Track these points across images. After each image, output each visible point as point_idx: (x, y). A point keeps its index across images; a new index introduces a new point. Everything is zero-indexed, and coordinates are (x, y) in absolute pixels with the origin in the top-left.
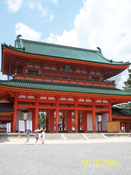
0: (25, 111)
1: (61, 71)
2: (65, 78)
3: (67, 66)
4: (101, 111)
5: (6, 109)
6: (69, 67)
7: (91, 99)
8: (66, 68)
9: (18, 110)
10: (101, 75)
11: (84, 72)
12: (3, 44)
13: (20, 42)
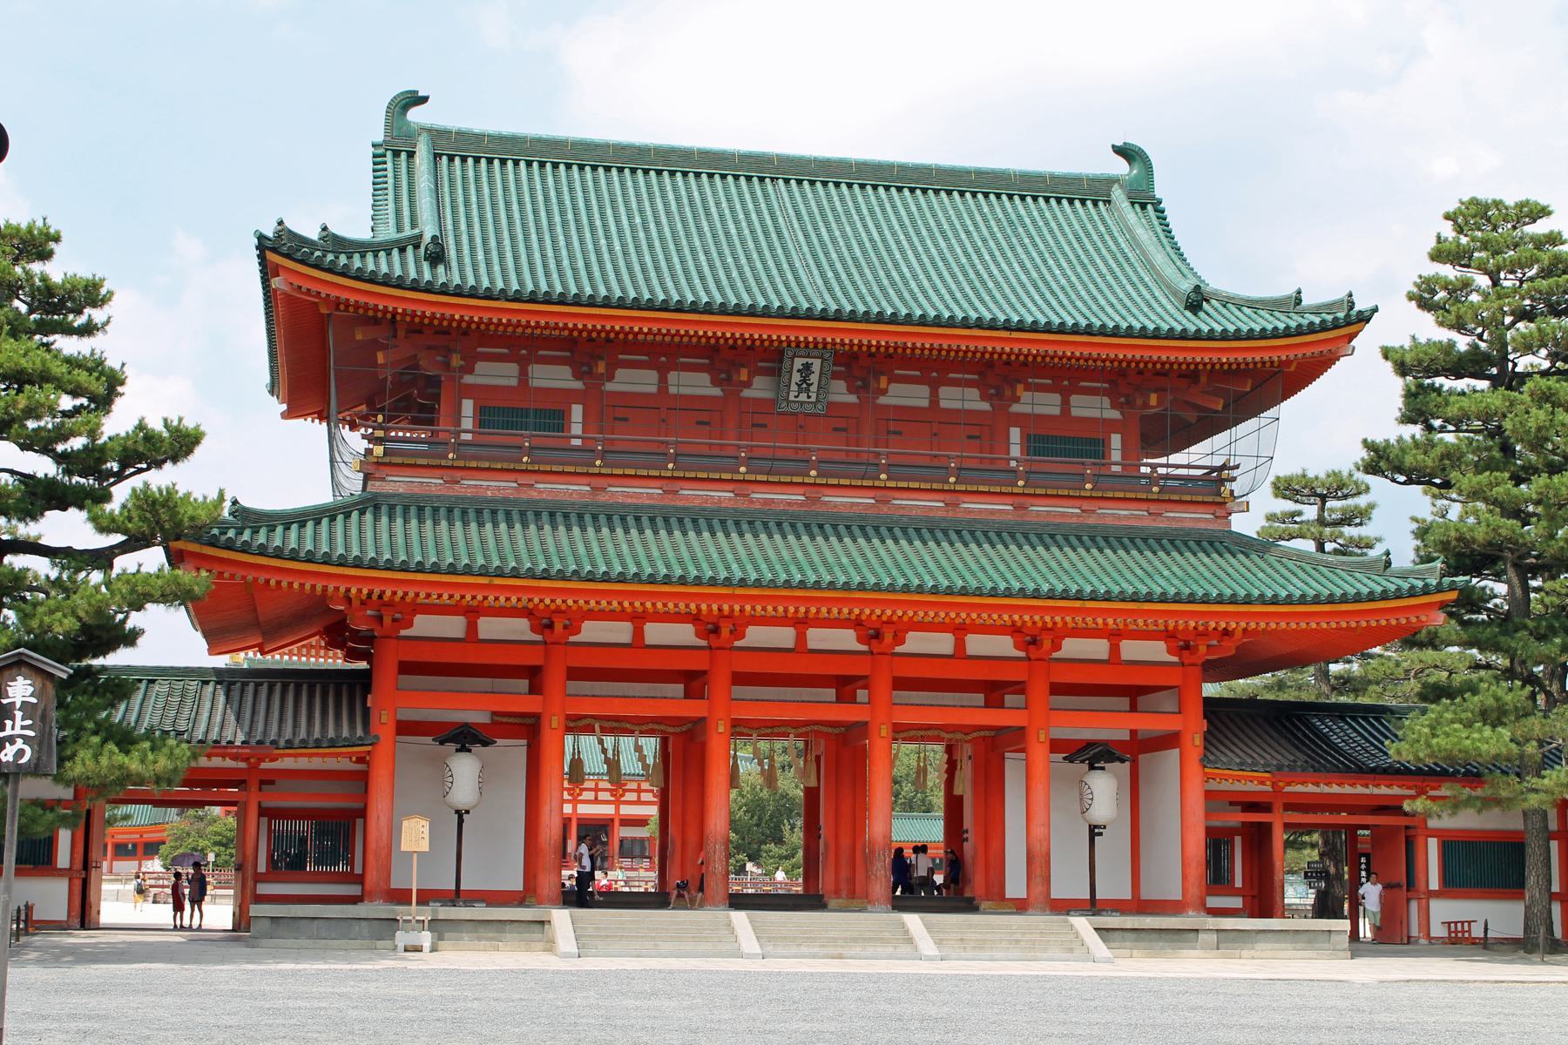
0: (465, 738)
1: (756, 400)
2: (774, 470)
3: (799, 363)
4: (1133, 733)
6: (816, 364)
8: (796, 377)
9: (406, 728)
10: (1115, 414)
11: (962, 398)
13: (411, 155)
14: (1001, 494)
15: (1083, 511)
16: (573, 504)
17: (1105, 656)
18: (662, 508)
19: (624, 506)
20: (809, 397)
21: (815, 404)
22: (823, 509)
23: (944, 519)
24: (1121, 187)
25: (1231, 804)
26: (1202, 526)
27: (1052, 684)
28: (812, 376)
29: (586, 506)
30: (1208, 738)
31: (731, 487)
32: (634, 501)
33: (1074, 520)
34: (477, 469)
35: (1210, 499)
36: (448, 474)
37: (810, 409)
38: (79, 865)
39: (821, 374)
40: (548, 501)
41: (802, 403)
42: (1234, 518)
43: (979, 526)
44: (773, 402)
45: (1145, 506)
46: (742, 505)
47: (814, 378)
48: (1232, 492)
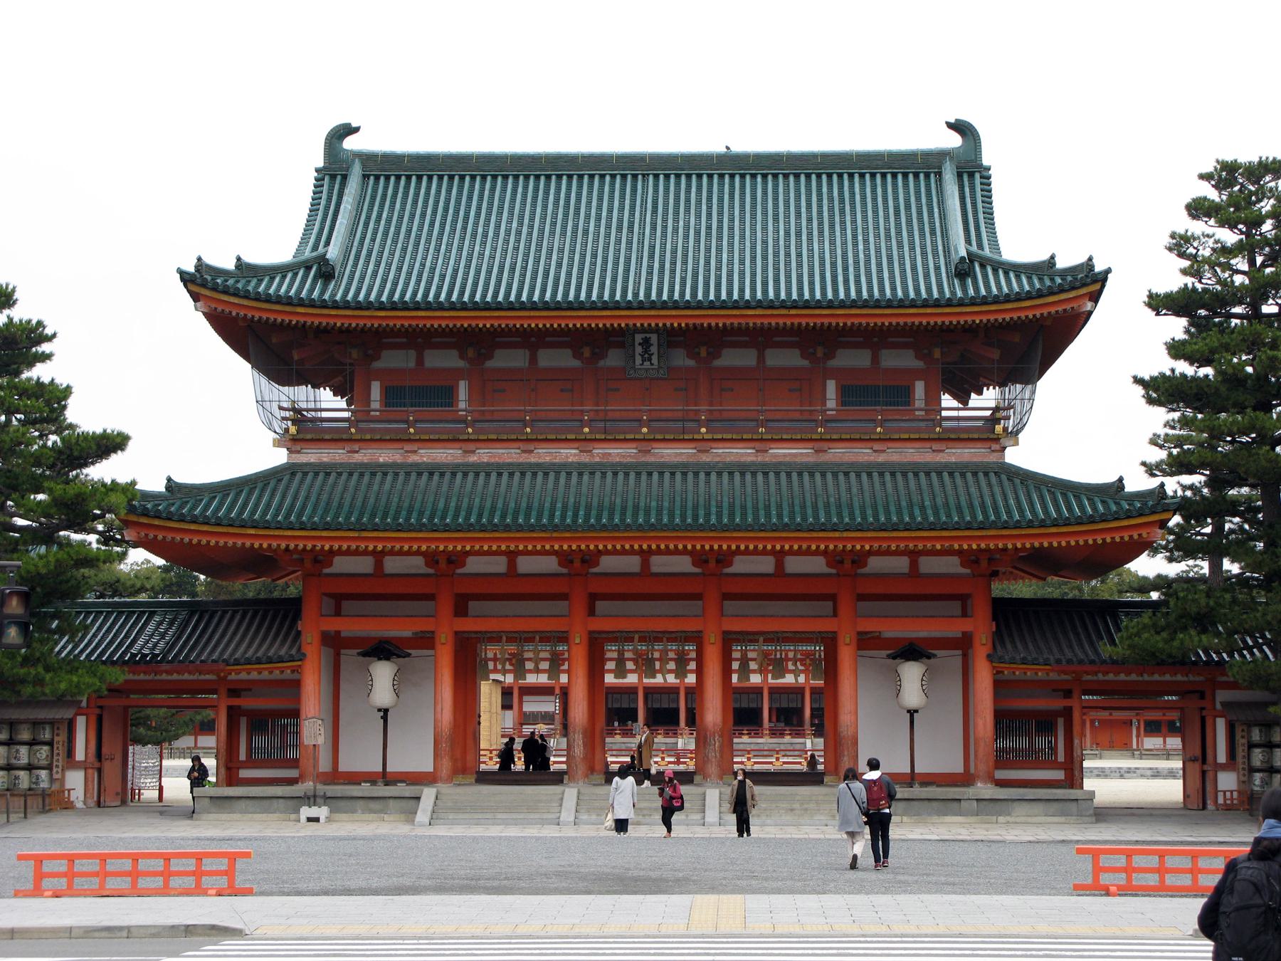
5: (271, 645)
6: (654, 338)
8: (639, 349)
11: (789, 358)
12: (191, 269)
16: (448, 464)
17: (906, 570)
18: (520, 464)
19: (488, 464)
20: (652, 364)
21: (658, 370)
22: (652, 459)
23: (753, 463)
24: (952, 159)
25: (1054, 690)
26: (980, 459)
27: (858, 595)
28: (652, 348)
29: (458, 465)
30: (998, 638)
31: (576, 445)
34: (371, 440)
35: (985, 436)
36: (348, 447)
38: (92, 758)
39: (659, 345)
40: (427, 464)
41: (647, 370)
42: (1008, 451)
43: (783, 467)
45: (928, 445)
46: (585, 458)
47: (654, 349)
48: (1005, 429)
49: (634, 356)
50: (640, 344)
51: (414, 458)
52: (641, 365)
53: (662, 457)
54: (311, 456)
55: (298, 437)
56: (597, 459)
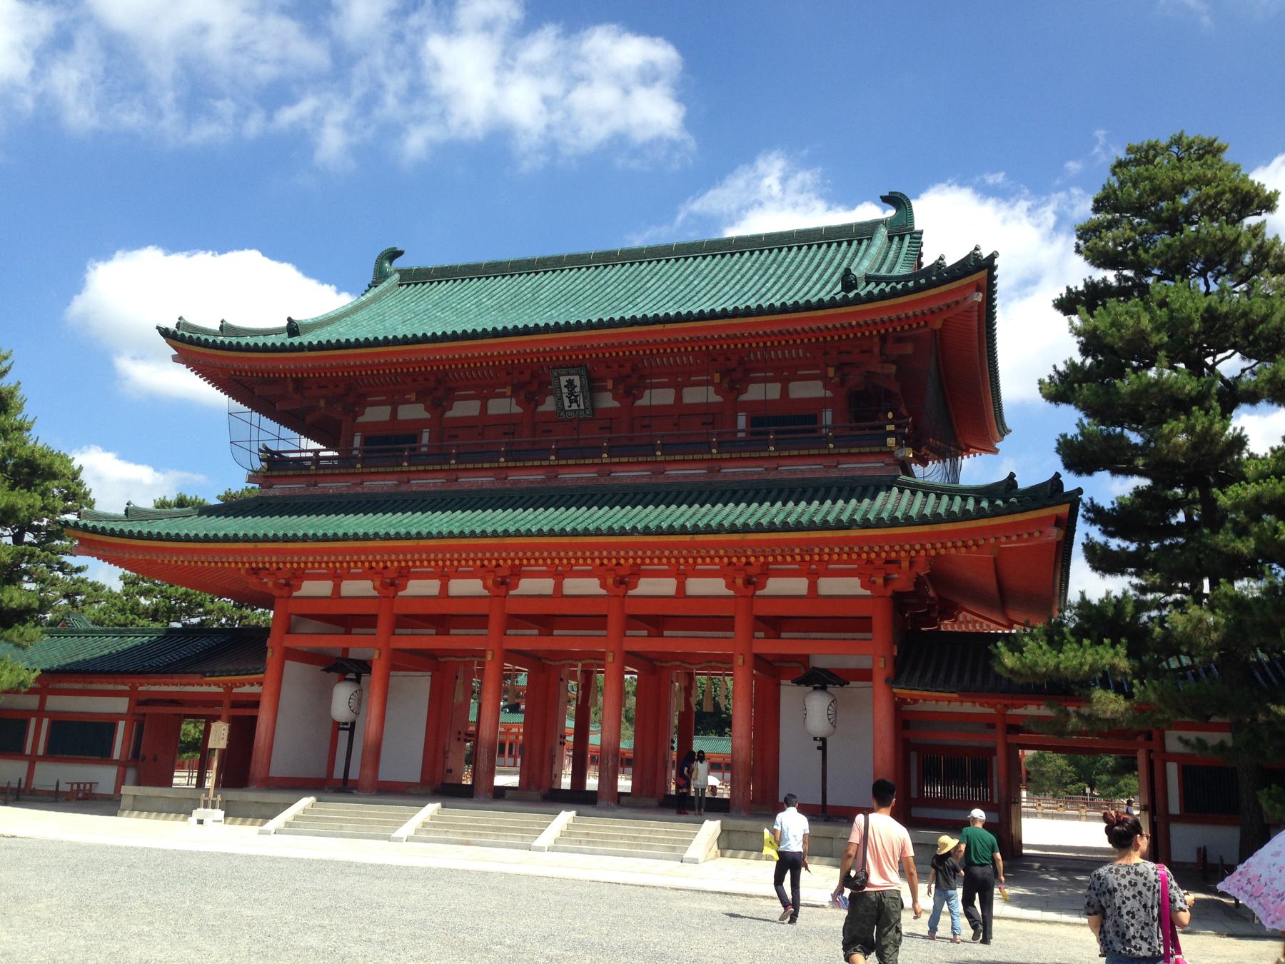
3: (564, 380)
7: (729, 572)
8: (565, 390)
14: (694, 460)
15: (766, 469)
26: (868, 473)
32: (424, 489)
33: (756, 477)
35: (877, 449)
37: (582, 415)
39: (582, 387)
40: (364, 494)
41: (575, 411)
44: (555, 413)
46: (499, 485)
49: (561, 399)
50: (565, 386)
51: (359, 489)
52: (570, 407)
53: (565, 481)
54: (278, 489)
55: (269, 474)
56: (508, 486)
